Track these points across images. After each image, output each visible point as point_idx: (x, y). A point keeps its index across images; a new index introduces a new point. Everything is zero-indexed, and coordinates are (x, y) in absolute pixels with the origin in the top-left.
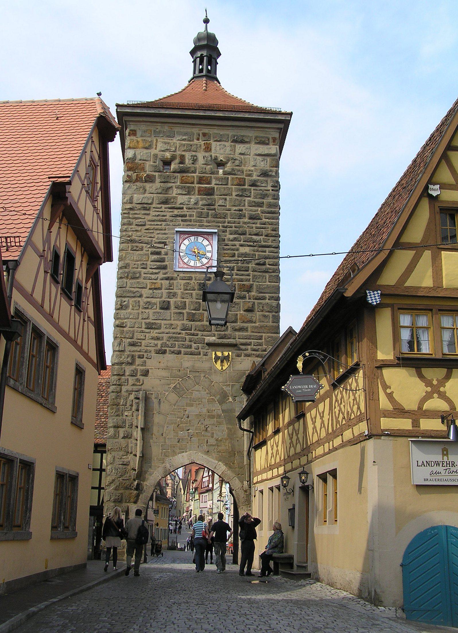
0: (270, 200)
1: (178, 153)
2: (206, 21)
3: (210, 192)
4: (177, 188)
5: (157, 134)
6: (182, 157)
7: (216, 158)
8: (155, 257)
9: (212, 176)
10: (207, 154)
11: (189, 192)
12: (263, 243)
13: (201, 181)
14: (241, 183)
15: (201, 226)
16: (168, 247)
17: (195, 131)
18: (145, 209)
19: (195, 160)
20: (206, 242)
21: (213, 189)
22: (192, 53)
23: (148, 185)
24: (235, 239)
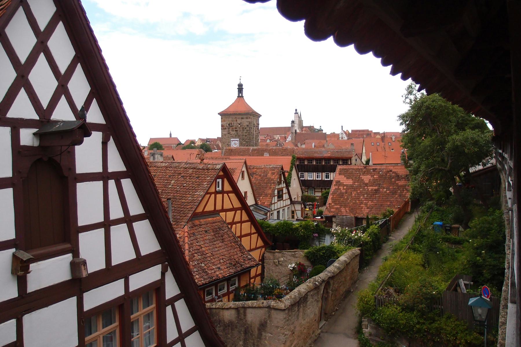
0: (248, 132)
1: (231, 122)
2: (240, 79)
3: (236, 131)
4: (231, 130)
5: (226, 118)
6: (231, 123)
7: (238, 123)
8: (228, 145)
9: (238, 127)
10: (236, 122)
11: (233, 131)
12: (248, 141)
13: (235, 128)
14: (243, 128)
15: (236, 138)
16: (230, 143)
17: (234, 117)
18: (225, 135)
19: (234, 123)
20: (237, 142)
21: (238, 130)
22: (238, 89)
23: (225, 130)
24: (242, 141)
